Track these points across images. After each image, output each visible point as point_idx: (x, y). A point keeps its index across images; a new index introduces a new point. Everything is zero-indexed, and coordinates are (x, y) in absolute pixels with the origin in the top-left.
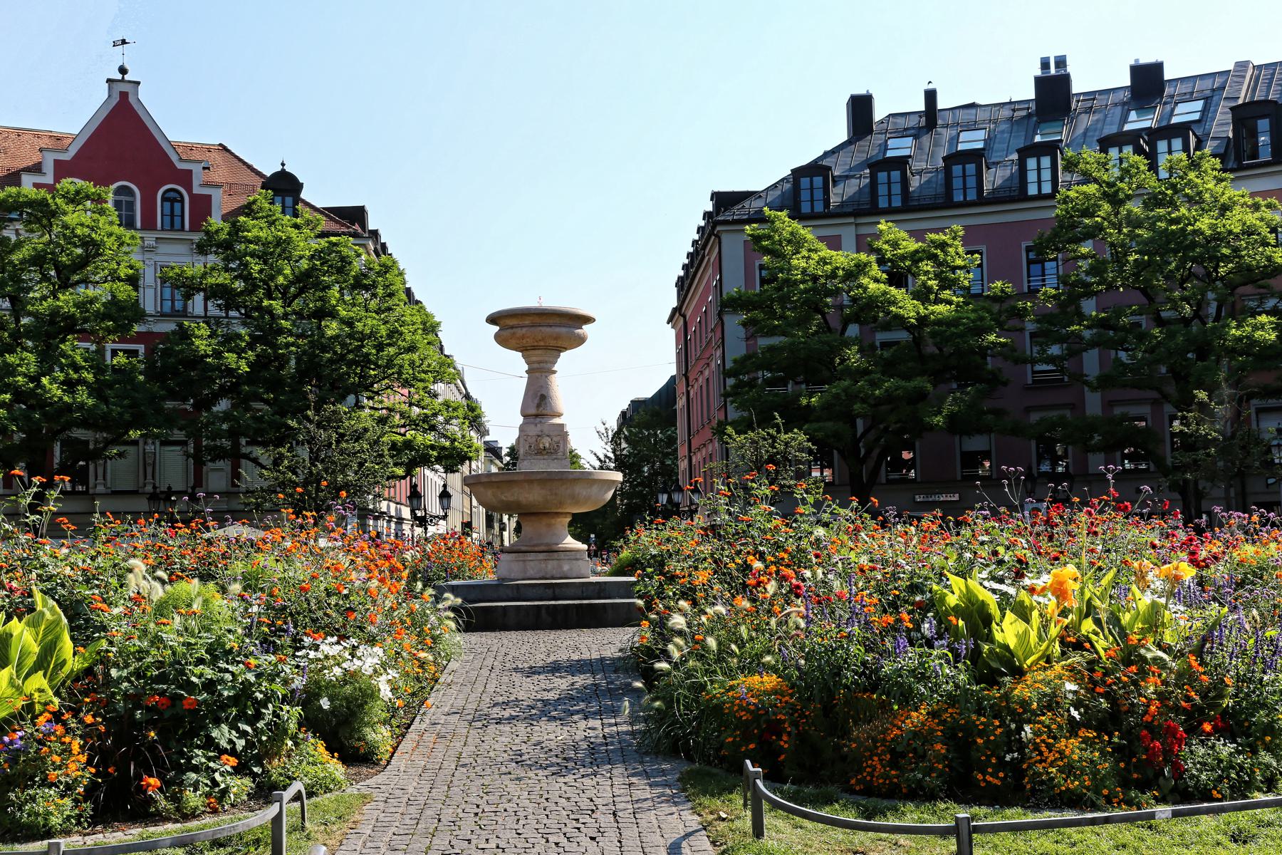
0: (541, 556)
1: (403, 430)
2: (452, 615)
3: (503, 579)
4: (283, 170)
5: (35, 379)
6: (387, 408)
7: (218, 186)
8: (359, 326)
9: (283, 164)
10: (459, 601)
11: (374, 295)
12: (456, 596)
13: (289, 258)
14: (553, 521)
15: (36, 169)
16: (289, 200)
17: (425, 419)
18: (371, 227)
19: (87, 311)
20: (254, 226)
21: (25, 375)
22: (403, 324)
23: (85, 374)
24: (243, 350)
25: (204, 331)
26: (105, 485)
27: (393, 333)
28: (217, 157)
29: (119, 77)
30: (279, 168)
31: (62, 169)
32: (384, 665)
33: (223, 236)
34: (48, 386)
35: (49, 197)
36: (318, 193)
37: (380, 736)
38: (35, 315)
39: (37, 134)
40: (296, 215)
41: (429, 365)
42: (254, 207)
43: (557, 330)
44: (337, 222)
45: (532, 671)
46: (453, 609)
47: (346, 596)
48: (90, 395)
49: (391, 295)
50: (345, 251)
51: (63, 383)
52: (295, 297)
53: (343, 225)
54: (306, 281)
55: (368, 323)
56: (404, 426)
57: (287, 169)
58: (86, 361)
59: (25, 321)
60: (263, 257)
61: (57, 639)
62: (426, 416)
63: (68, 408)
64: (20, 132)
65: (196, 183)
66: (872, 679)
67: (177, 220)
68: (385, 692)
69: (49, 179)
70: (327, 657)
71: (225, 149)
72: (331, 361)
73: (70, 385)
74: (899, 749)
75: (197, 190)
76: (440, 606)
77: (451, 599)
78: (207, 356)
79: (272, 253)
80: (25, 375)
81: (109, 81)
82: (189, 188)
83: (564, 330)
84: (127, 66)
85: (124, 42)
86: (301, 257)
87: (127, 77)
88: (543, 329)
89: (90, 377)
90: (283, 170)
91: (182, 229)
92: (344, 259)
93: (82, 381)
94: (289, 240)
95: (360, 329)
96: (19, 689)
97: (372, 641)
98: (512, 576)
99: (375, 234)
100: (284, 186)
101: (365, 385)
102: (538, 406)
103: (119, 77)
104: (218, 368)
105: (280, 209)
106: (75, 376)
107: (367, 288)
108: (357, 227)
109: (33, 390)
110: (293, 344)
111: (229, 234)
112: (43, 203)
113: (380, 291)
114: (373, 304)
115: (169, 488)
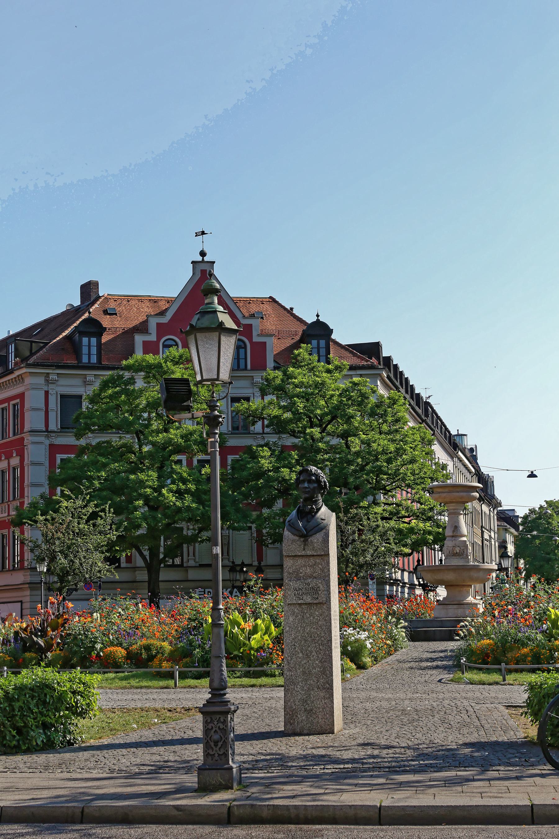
0: (455, 606)
1: (406, 520)
2: (404, 630)
3: (436, 618)
4: (318, 320)
5: (157, 490)
6: (396, 504)
7: (271, 335)
8: (374, 445)
9: (318, 316)
10: (406, 624)
11: (385, 421)
12: (405, 622)
13: (324, 397)
14: (461, 589)
15: (142, 328)
16: (323, 343)
17: (423, 512)
18: (385, 354)
19: (189, 441)
20: (299, 374)
21: (150, 487)
22: (406, 443)
23: (190, 486)
24: (294, 466)
25: (266, 452)
26: (195, 560)
27: (399, 452)
28: (267, 308)
29: (200, 259)
30: (315, 319)
31: (162, 329)
32: (369, 637)
33: (278, 381)
34: (166, 494)
35: (162, 361)
36: (343, 335)
37: (367, 660)
38: (154, 444)
39: (140, 299)
40: (329, 363)
41: (425, 473)
42: (299, 358)
43: (462, 494)
44: (359, 357)
45: (434, 652)
46: (404, 627)
47: (356, 616)
48: (193, 501)
49: (397, 421)
50: (364, 389)
51: (176, 492)
52: (330, 422)
53: (363, 359)
54: (336, 413)
55: (381, 443)
56: (409, 517)
57: (321, 319)
58: (190, 476)
59: (145, 449)
60: (306, 397)
61: (270, 625)
62: (424, 510)
63: (179, 510)
64: (129, 298)
65: (255, 333)
66: (517, 641)
67: (242, 362)
68: (369, 646)
69: (153, 337)
70: (350, 634)
71: (272, 300)
72: (355, 471)
73: (180, 494)
74: (519, 659)
75: (255, 339)
76: (399, 626)
77: (403, 623)
78: (269, 471)
79: (312, 394)
80: (150, 487)
81: (193, 262)
82: (250, 338)
83: (464, 494)
84: (206, 250)
85: (203, 233)
86: (332, 396)
87: (206, 259)
88: (454, 494)
89: (192, 487)
90: (318, 320)
91: (246, 369)
92: (364, 396)
93: (188, 491)
94: (323, 384)
95: (375, 448)
96: (263, 639)
97: (364, 631)
98: (441, 616)
99: (388, 360)
100: (319, 332)
101: (379, 487)
102: (453, 531)
103: (200, 259)
104: (277, 479)
105: (317, 358)
106: (183, 487)
107: (382, 416)
108: (374, 361)
109: (157, 498)
110: (327, 460)
111: (282, 380)
112: (159, 366)
113: (390, 419)
114: (385, 427)
115: (243, 563)
